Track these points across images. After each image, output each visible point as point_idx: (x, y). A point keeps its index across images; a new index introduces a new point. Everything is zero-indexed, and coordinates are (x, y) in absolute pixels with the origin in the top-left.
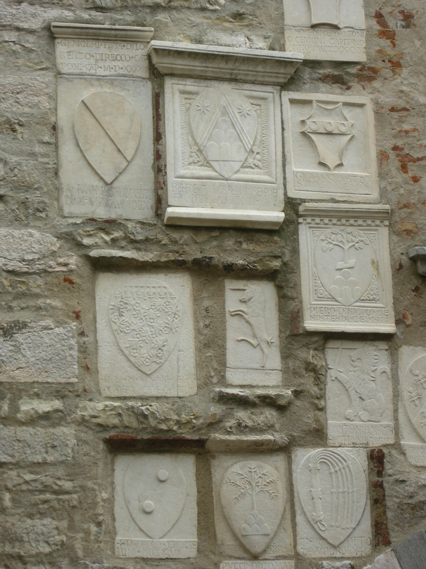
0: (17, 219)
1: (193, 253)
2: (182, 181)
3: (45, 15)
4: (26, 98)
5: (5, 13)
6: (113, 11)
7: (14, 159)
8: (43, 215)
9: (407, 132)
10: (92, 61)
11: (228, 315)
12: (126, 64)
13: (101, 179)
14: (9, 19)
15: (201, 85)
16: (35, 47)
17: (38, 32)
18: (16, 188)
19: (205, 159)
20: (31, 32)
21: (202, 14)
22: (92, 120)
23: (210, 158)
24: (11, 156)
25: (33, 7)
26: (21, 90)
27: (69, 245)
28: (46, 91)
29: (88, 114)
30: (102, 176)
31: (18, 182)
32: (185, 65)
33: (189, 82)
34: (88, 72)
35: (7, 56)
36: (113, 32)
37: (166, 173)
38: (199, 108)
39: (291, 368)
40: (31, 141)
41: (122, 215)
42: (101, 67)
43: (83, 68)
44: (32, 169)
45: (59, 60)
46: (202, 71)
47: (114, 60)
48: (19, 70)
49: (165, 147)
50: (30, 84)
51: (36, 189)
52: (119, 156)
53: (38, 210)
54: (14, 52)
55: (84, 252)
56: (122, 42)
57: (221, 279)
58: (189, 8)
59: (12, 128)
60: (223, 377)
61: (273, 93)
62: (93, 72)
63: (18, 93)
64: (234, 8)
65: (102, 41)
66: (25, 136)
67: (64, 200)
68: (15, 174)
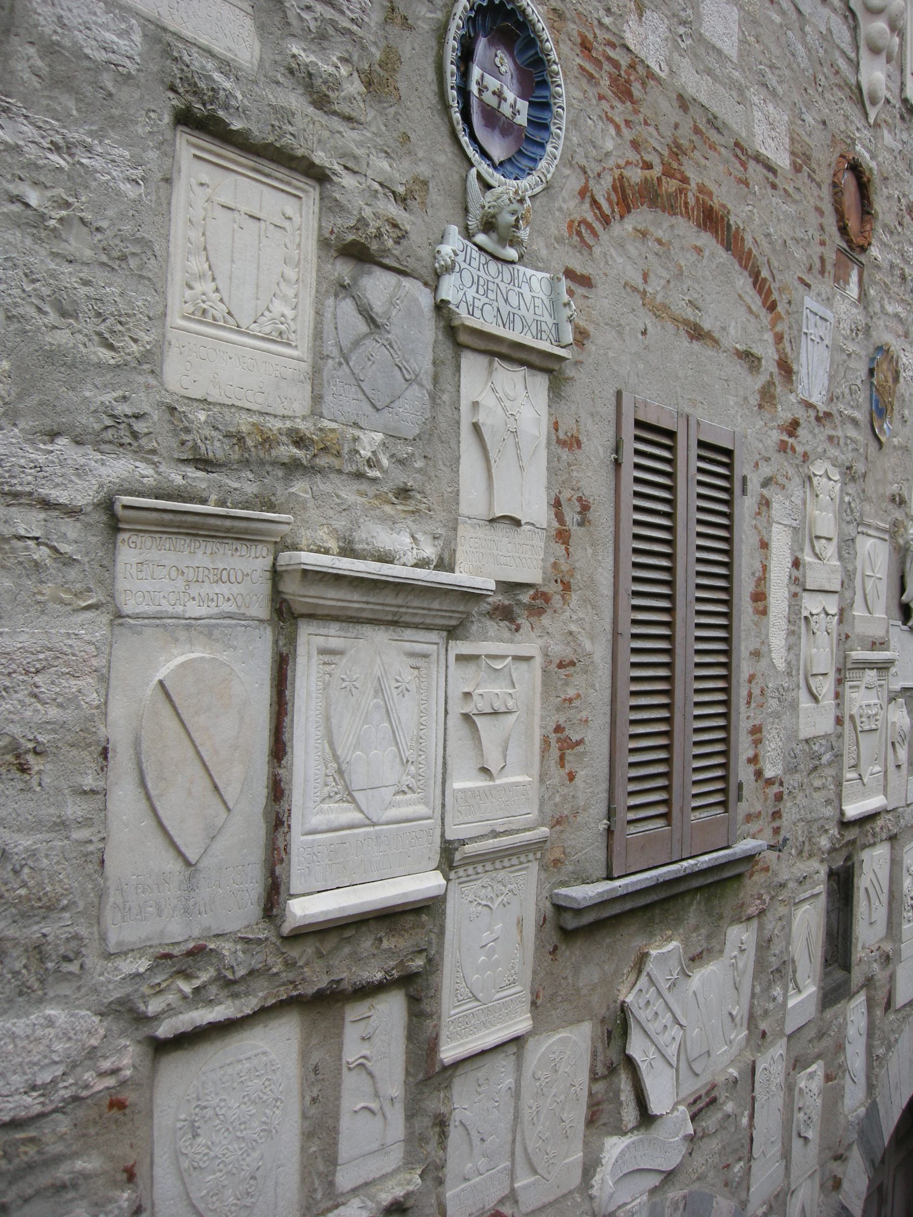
0: (23, 991)
1: (317, 980)
2: (314, 840)
3: (103, 471)
4: (53, 683)
5: (22, 462)
6: (224, 469)
7: (24, 842)
8: (74, 967)
9: (570, 700)
10: (180, 583)
11: (345, 1070)
12: (236, 589)
13: (181, 854)
14: (30, 478)
15: (349, 635)
16: (80, 552)
17: (86, 514)
18: (24, 915)
19: (346, 787)
20: (72, 512)
21: (356, 485)
22: (175, 724)
23: (355, 786)
24: (16, 836)
25: (81, 450)
26: (44, 663)
27: (122, 1024)
28: (95, 662)
29: (167, 711)
30: (183, 849)
31: (29, 900)
32: (338, 600)
33: (333, 629)
34: (170, 609)
35: (20, 576)
36: (228, 523)
37: (289, 826)
38: (344, 685)
39: (418, 1131)
40: (58, 790)
41: (210, 928)
42: (194, 599)
43: (163, 602)
44: (58, 863)
45: (122, 584)
46: (358, 609)
47: (217, 582)
48: (43, 612)
49: (290, 771)
50: (65, 649)
51: (64, 909)
52: (214, 800)
53: (67, 959)
54: (36, 564)
55: (146, 1031)
56: (235, 542)
57: (339, 1005)
58: (339, 472)
59: (20, 764)
60: (331, 1184)
61: (437, 644)
62: (179, 609)
63: (37, 672)
64: (401, 477)
65: (201, 539)
66: (47, 780)
67: (110, 915)
68: (23, 881)
